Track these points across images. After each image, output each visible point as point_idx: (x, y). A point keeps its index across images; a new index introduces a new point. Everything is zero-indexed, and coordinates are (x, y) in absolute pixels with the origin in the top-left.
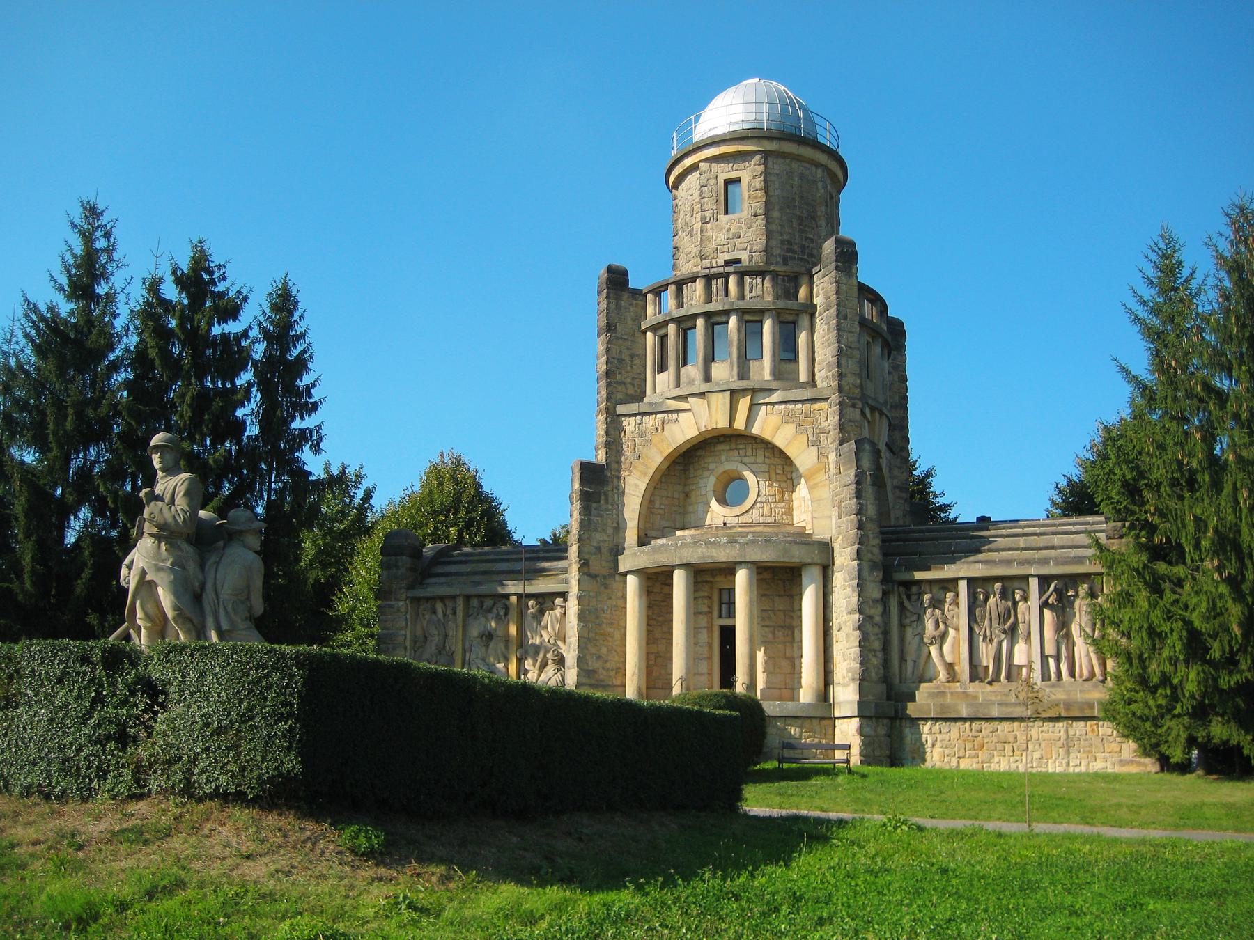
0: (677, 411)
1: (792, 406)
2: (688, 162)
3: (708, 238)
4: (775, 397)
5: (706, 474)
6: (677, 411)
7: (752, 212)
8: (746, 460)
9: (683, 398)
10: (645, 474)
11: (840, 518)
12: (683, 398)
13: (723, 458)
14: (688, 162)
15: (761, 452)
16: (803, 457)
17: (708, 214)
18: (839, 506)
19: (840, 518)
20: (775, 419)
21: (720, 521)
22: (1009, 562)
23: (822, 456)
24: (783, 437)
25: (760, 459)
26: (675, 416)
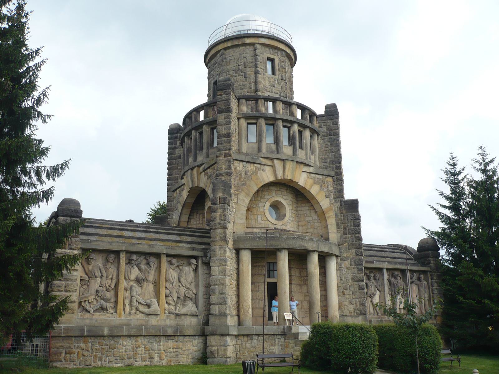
0: (264, 165)
1: (317, 176)
2: (248, 41)
3: (261, 82)
4: (311, 170)
5: (263, 200)
6: (264, 165)
7: (280, 78)
8: (285, 197)
9: (272, 159)
10: (248, 195)
11: (345, 234)
12: (272, 159)
13: (274, 194)
14: (248, 41)
15: (290, 195)
16: (325, 203)
17: (260, 70)
18: (345, 229)
19: (345, 234)
20: (310, 181)
21: (273, 226)
22: (396, 263)
23: (331, 203)
24: (314, 190)
25: (290, 198)
26: (263, 167)
